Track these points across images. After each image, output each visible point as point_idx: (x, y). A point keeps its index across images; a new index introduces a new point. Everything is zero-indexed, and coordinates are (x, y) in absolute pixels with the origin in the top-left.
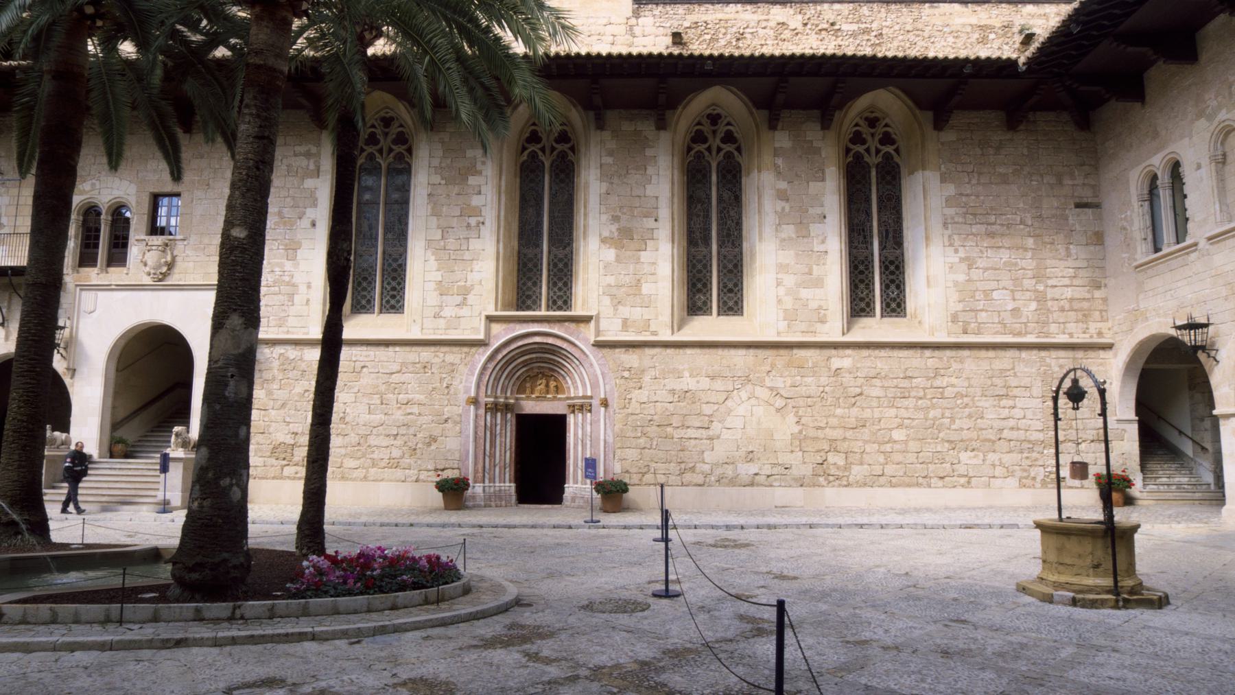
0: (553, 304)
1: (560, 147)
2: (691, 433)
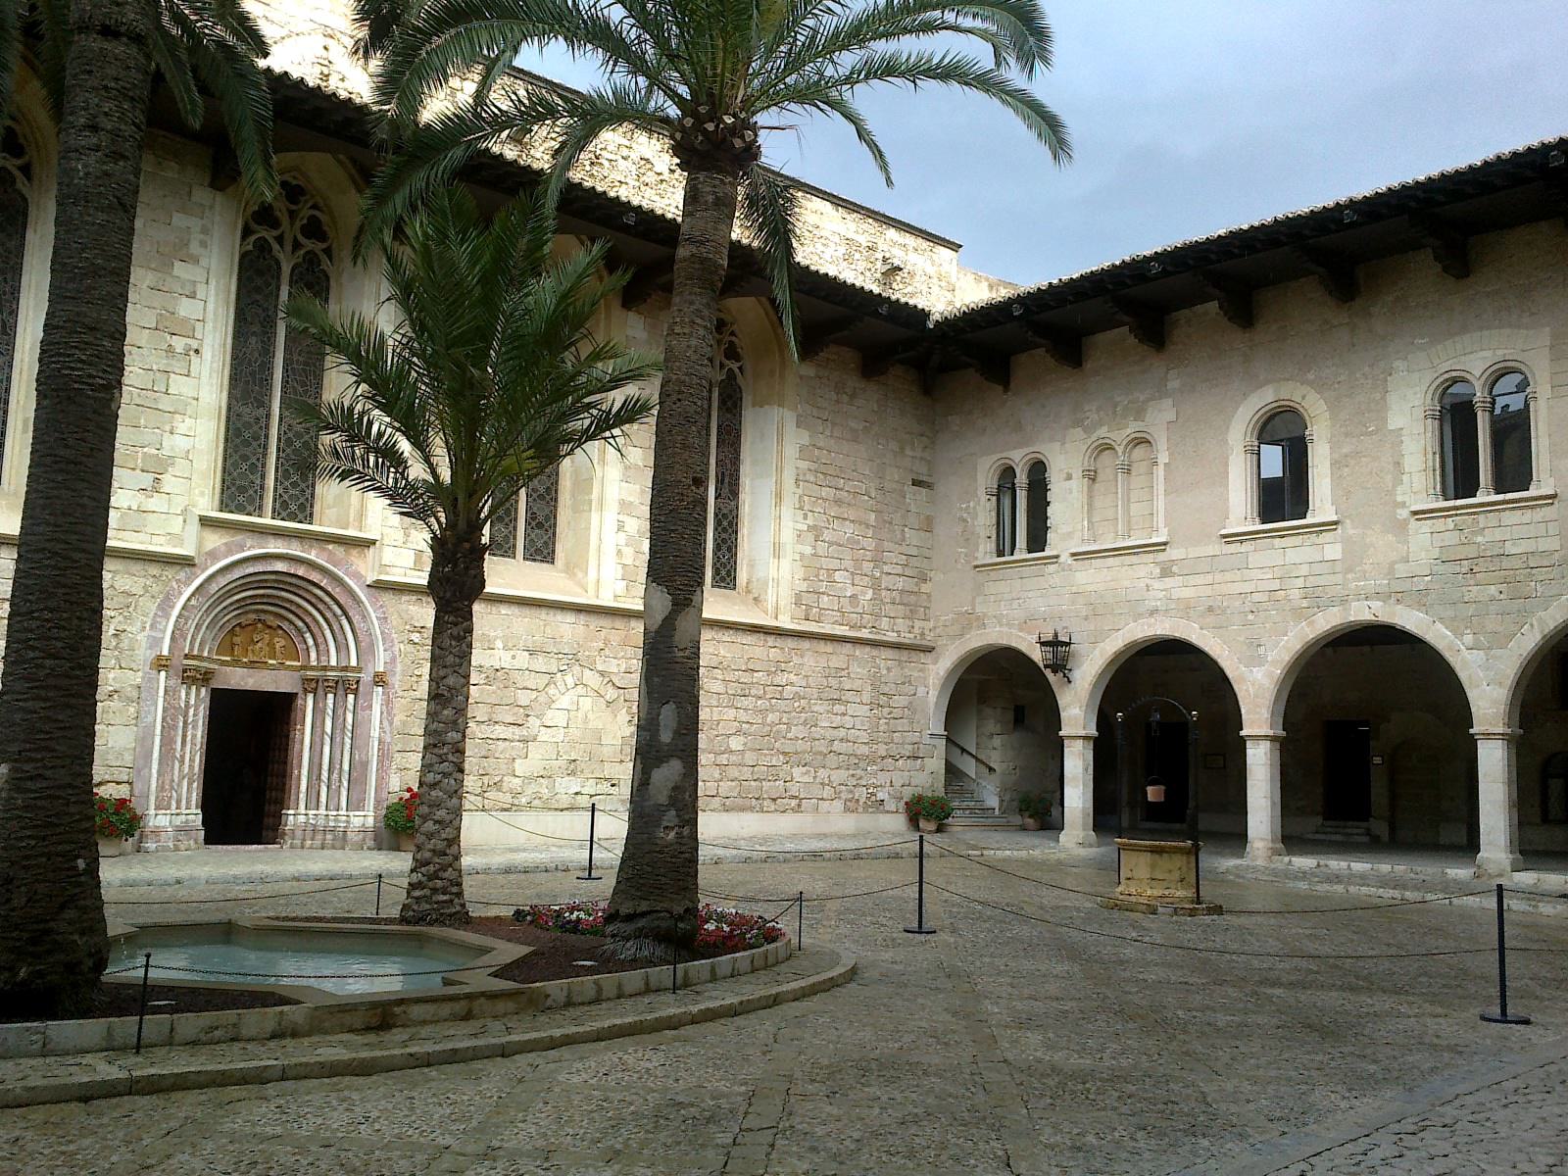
0: (281, 510)
1: (309, 245)
2: (500, 731)
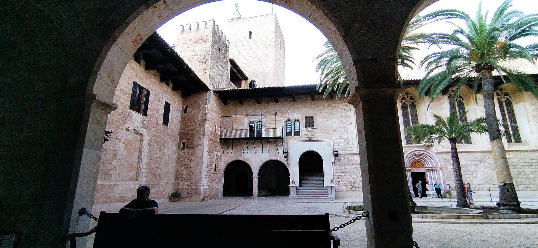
1: (411, 101)
